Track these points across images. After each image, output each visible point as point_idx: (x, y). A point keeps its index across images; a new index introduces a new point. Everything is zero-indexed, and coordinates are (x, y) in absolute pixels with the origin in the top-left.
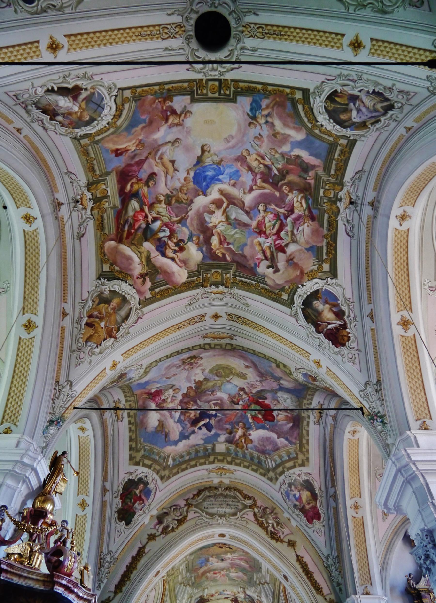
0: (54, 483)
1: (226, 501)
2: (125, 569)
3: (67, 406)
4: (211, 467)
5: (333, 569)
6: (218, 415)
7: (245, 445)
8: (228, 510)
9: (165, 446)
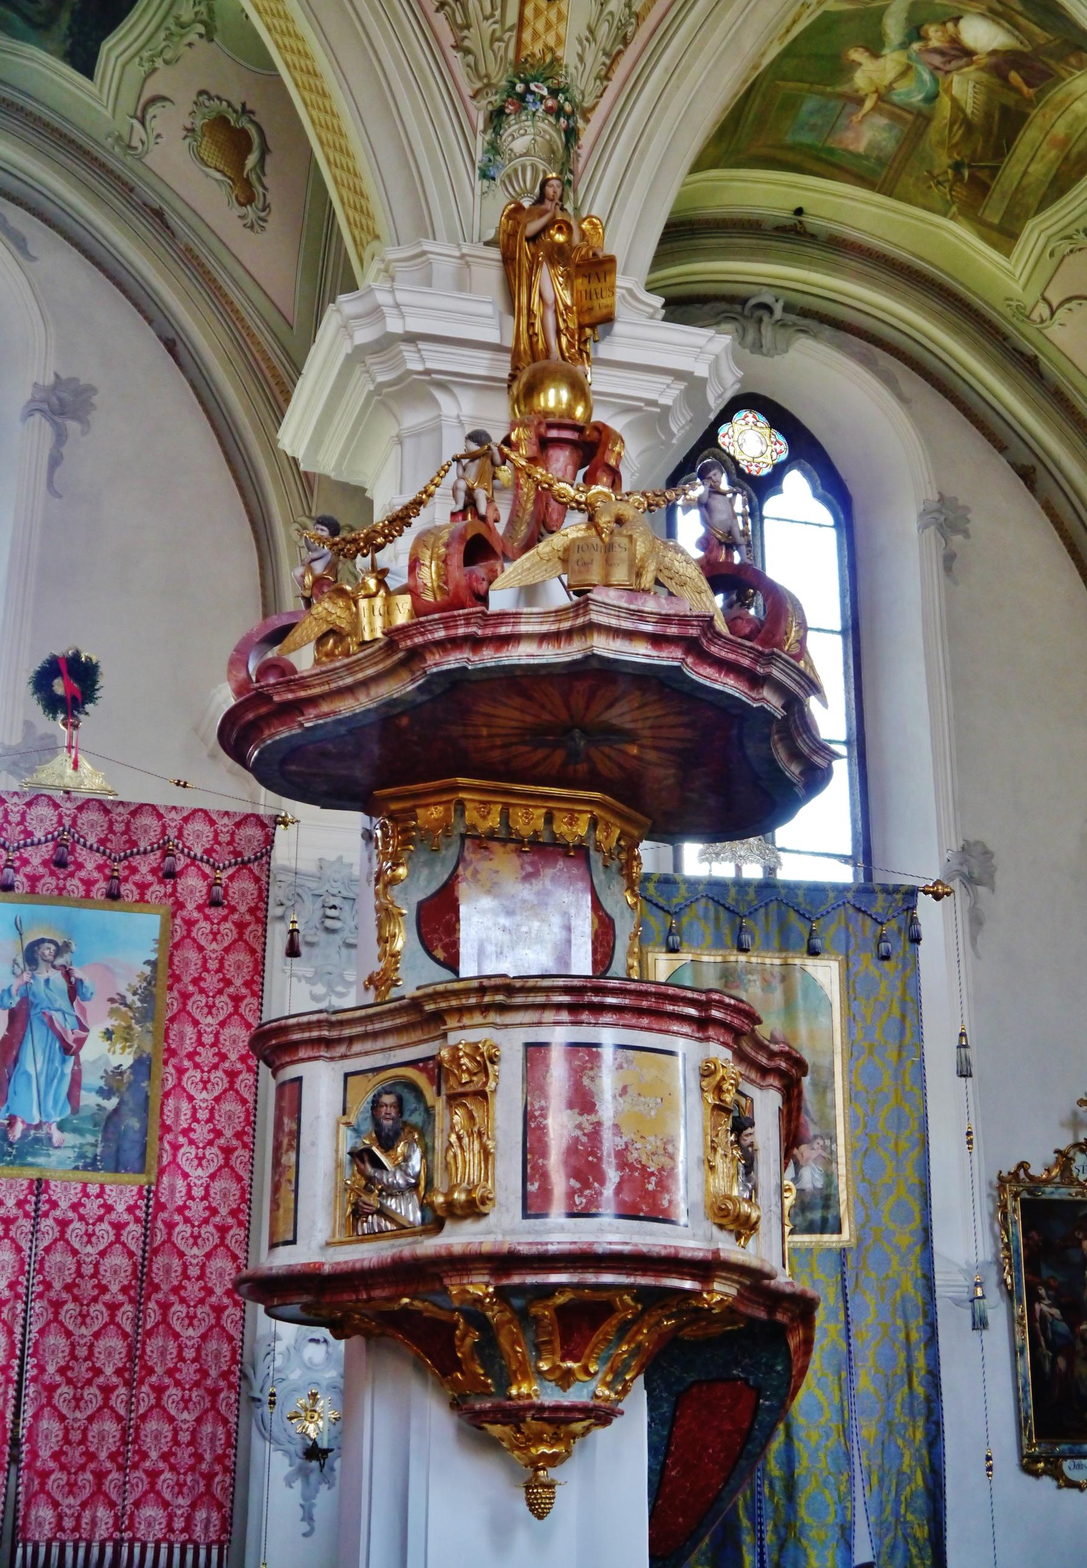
3: (512, 18)
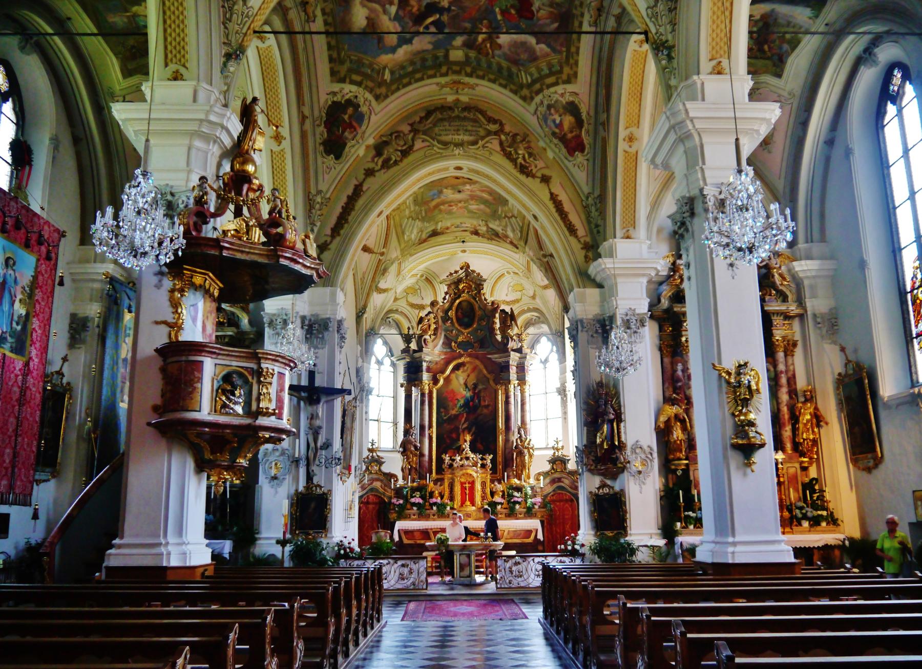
0: (250, 140)
1: (463, 126)
2: (341, 210)
3: (244, 31)
4: (443, 80)
5: (593, 209)
6: (453, 8)
7: (490, 51)
8: (466, 138)
9: (379, 55)
